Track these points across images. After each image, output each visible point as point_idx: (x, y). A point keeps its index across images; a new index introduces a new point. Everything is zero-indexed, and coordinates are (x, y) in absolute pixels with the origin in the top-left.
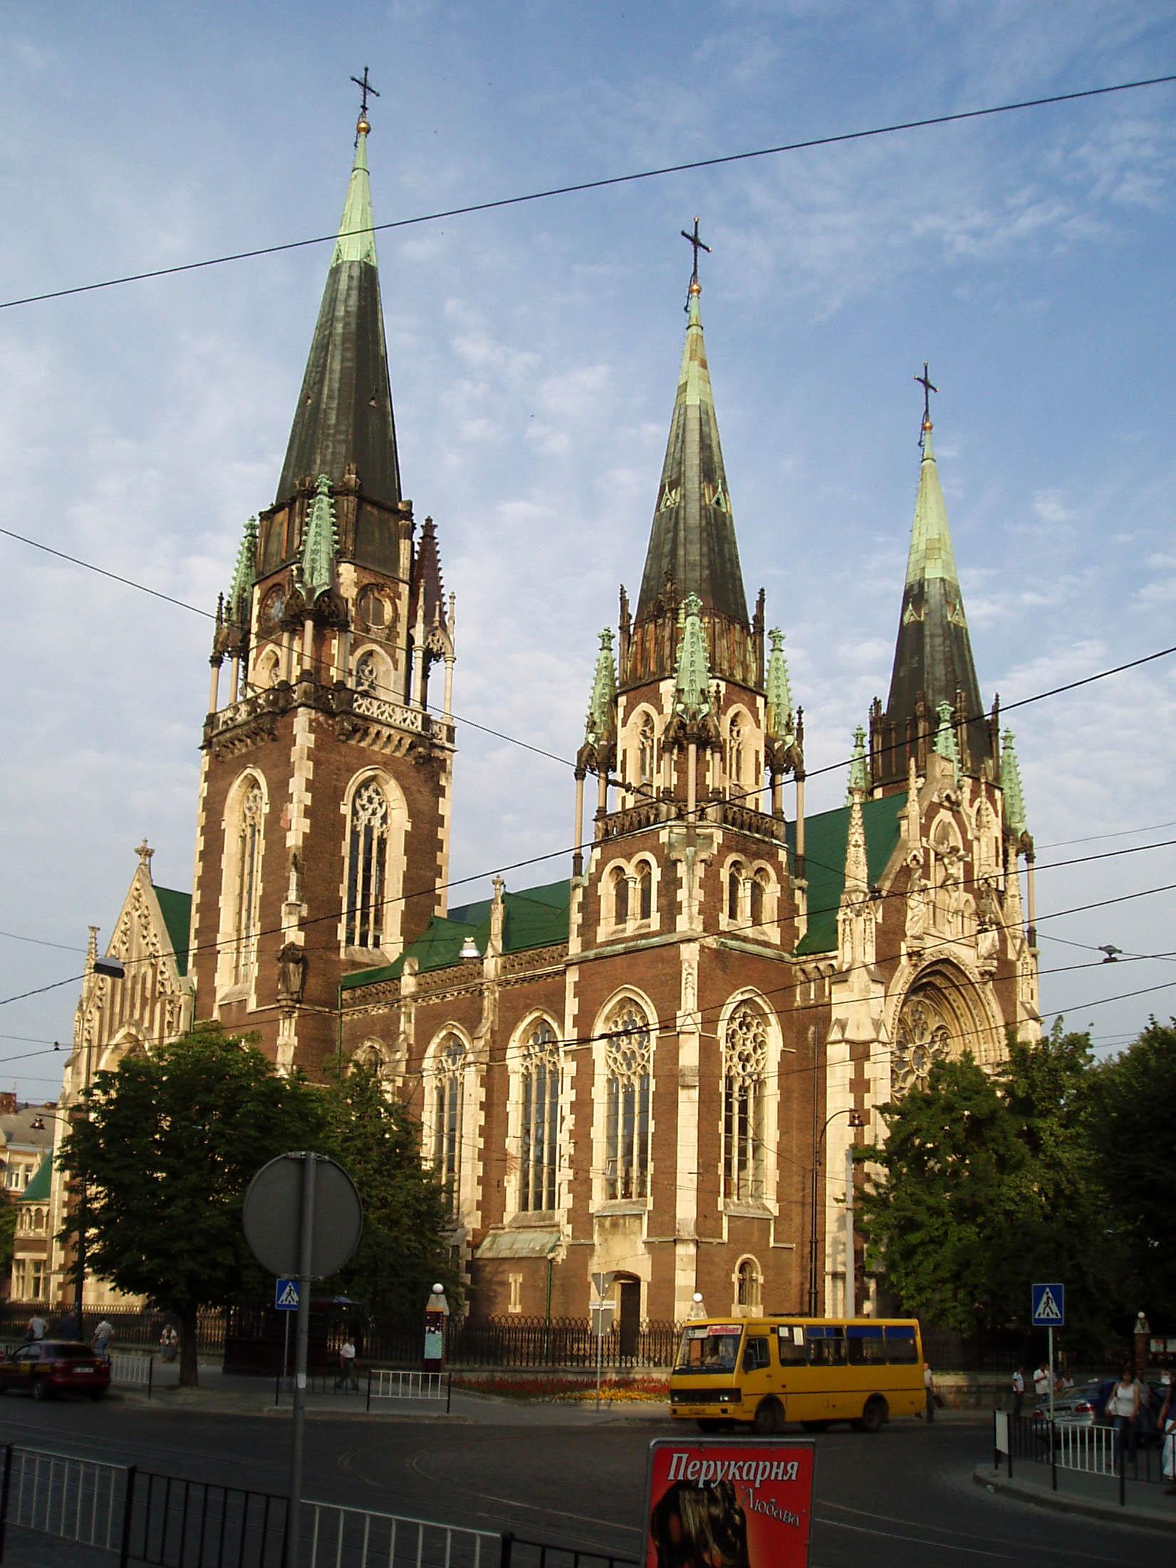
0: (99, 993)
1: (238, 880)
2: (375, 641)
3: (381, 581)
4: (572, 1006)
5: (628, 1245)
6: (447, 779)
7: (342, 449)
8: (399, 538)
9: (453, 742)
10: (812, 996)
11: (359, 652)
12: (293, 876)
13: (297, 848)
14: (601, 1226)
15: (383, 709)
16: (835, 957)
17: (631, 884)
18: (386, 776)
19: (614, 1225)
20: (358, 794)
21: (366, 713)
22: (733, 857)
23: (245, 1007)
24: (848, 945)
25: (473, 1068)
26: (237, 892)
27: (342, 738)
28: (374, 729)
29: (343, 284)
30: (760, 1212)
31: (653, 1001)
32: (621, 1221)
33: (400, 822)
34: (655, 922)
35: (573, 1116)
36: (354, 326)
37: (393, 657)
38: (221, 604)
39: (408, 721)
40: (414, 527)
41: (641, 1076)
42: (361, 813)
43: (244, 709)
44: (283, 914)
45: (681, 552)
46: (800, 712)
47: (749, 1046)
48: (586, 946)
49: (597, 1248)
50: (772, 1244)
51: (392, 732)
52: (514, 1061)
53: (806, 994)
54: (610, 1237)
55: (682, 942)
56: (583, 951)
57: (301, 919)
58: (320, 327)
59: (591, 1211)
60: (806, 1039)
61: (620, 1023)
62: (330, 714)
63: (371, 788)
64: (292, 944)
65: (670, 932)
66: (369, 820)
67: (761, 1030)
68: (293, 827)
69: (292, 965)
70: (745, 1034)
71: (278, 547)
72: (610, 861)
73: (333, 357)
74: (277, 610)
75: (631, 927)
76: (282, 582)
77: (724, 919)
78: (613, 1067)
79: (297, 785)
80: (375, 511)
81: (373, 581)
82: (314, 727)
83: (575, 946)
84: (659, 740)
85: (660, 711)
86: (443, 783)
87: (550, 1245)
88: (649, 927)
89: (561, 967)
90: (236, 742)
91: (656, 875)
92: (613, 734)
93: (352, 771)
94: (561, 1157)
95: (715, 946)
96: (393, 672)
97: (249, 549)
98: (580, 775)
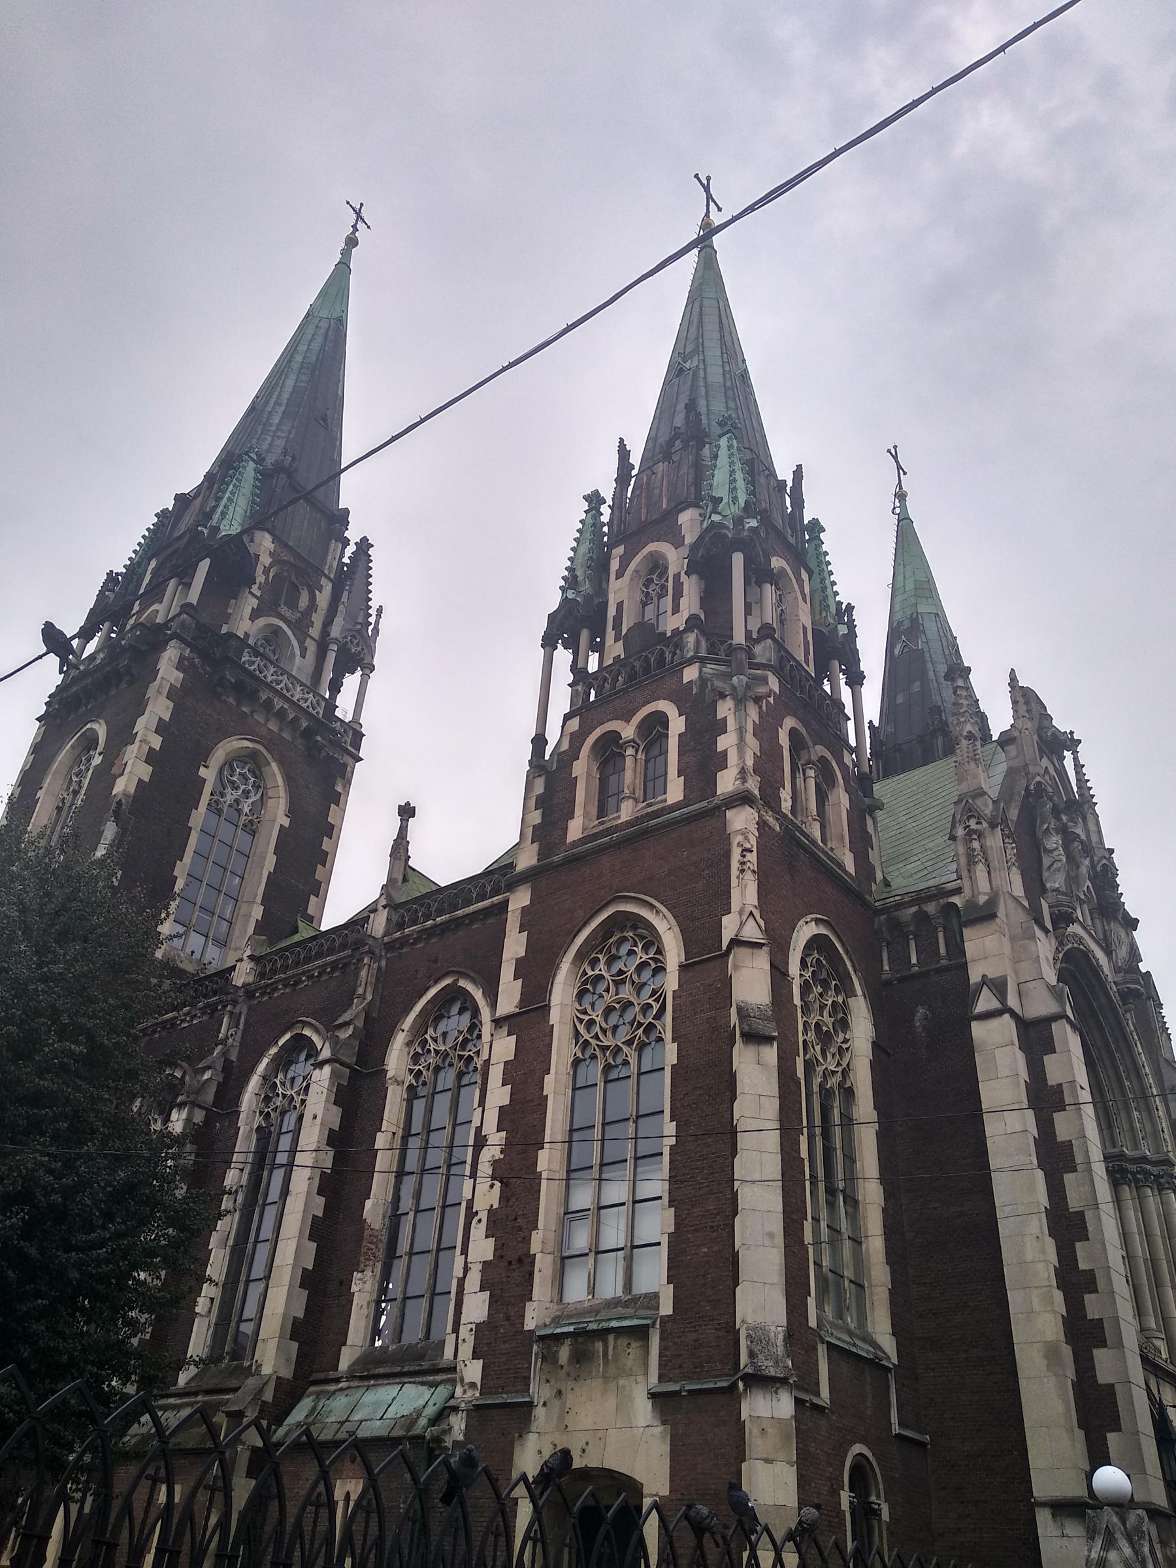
4: (515, 945)
5: (611, 1402)
10: (914, 960)
11: (262, 622)
12: (110, 830)
13: (125, 794)
14: (549, 1358)
15: (280, 678)
17: (630, 751)
18: (268, 756)
19: (581, 1357)
20: (229, 764)
24: (980, 870)
25: (327, 1069)
27: (219, 689)
32: (599, 1345)
33: (278, 814)
34: (675, 791)
37: (301, 644)
39: (309, 703)
40: (346, 542)
42: (229, 790)
45: (702, 403)
49: (539, 1412)
52: (396, 1060)
54: (570, 1384)
56: (539, 860)
59: (530, 1324)
66: (237, 801)
68: (128, 770)
70: (821, 995)
79: (144, 725)
81: (292, 560)
85: (678, 543)
86: (339, 788)
87: (430, 1411)
88: (665, 801)
91: (677, 725)
92: (601, 590)
96: (298, 659)
98: (549, 642)
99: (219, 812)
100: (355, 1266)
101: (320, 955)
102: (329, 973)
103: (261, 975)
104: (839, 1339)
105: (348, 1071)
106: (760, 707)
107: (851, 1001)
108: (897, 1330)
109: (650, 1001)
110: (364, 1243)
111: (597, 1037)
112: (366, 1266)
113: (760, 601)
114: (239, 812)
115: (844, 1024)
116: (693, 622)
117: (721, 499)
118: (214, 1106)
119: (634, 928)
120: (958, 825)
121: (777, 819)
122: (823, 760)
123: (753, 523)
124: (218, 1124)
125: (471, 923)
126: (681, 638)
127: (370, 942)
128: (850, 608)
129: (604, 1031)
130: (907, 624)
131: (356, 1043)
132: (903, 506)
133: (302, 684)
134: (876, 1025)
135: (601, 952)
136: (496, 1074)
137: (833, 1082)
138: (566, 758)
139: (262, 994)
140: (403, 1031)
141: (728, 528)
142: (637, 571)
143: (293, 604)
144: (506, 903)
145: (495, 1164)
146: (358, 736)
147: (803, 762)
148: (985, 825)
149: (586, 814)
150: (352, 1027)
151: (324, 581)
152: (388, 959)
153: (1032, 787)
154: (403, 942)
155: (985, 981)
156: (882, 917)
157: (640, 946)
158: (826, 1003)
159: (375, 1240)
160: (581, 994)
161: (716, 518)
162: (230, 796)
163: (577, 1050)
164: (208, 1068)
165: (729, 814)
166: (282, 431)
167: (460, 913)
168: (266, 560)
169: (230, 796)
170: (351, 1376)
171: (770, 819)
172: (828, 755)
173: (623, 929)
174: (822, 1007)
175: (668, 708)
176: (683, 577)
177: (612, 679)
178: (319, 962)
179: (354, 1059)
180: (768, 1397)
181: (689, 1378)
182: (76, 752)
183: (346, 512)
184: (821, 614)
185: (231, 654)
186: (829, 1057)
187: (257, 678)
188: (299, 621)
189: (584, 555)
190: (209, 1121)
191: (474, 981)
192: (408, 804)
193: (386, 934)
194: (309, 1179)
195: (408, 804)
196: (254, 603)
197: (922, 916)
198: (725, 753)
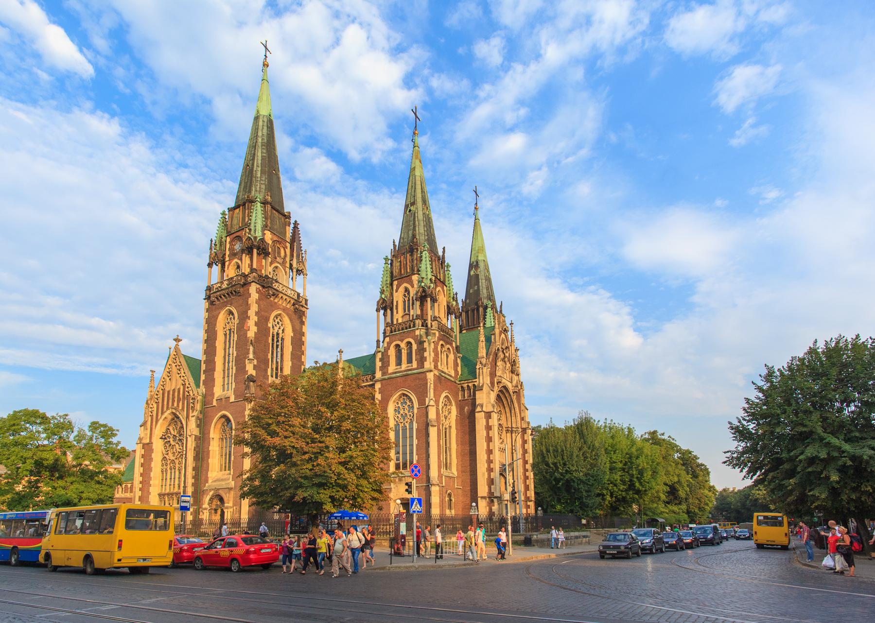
0: (156, 397)
1: (223, 351)
2: (278, 263)
3: (280, 240)
7: (263, 187)
8: (286, 225)
11: (273, 266)
12: (251, 348)
17: (403, 351)
23: (229, 400)
24: (481, 377)
26: (223, 355)
28: (281, 295)
29: (261, 123)
32: (404, 479)
34: (415, 364)
36: (266, 140)
38: (211, 243)
43: (226, 283)
44: (246, 363)
46: (456, 294)
47: (447, 413)
48: (384, 374)
49: (393, 489)
55: (427, 372)
57: (254, 366)
58: (251, 139)
60: (464, 411)
61: (400, 403)
62: (263, 287)
63: (278, 319)
64: (251, 375)
65: (421, 368)
69: (251, 383)
71: (237, 224)
73: (258, 151)
74: (238, 247)
75: (404, 366)
76: (241, 235)
77: (439, 364)
78: (397, 420)
79: (252, 312)
80: (277, 213)
82: (258, 291)
83: (378, 375)
84: (413, 297)
89: (371, 383)
90: (222, 296)
91: (415, 347)
95: (438, 374)
97: (223, 223)
98: (378, 310)
113: (434, 306)
138: (387, 349)
143: (279, 253)
155: (478, 405)
165: (427, 374)
168: (270, 242)
182: (225, 315)
183: (289, 213)
187: (277, 291)
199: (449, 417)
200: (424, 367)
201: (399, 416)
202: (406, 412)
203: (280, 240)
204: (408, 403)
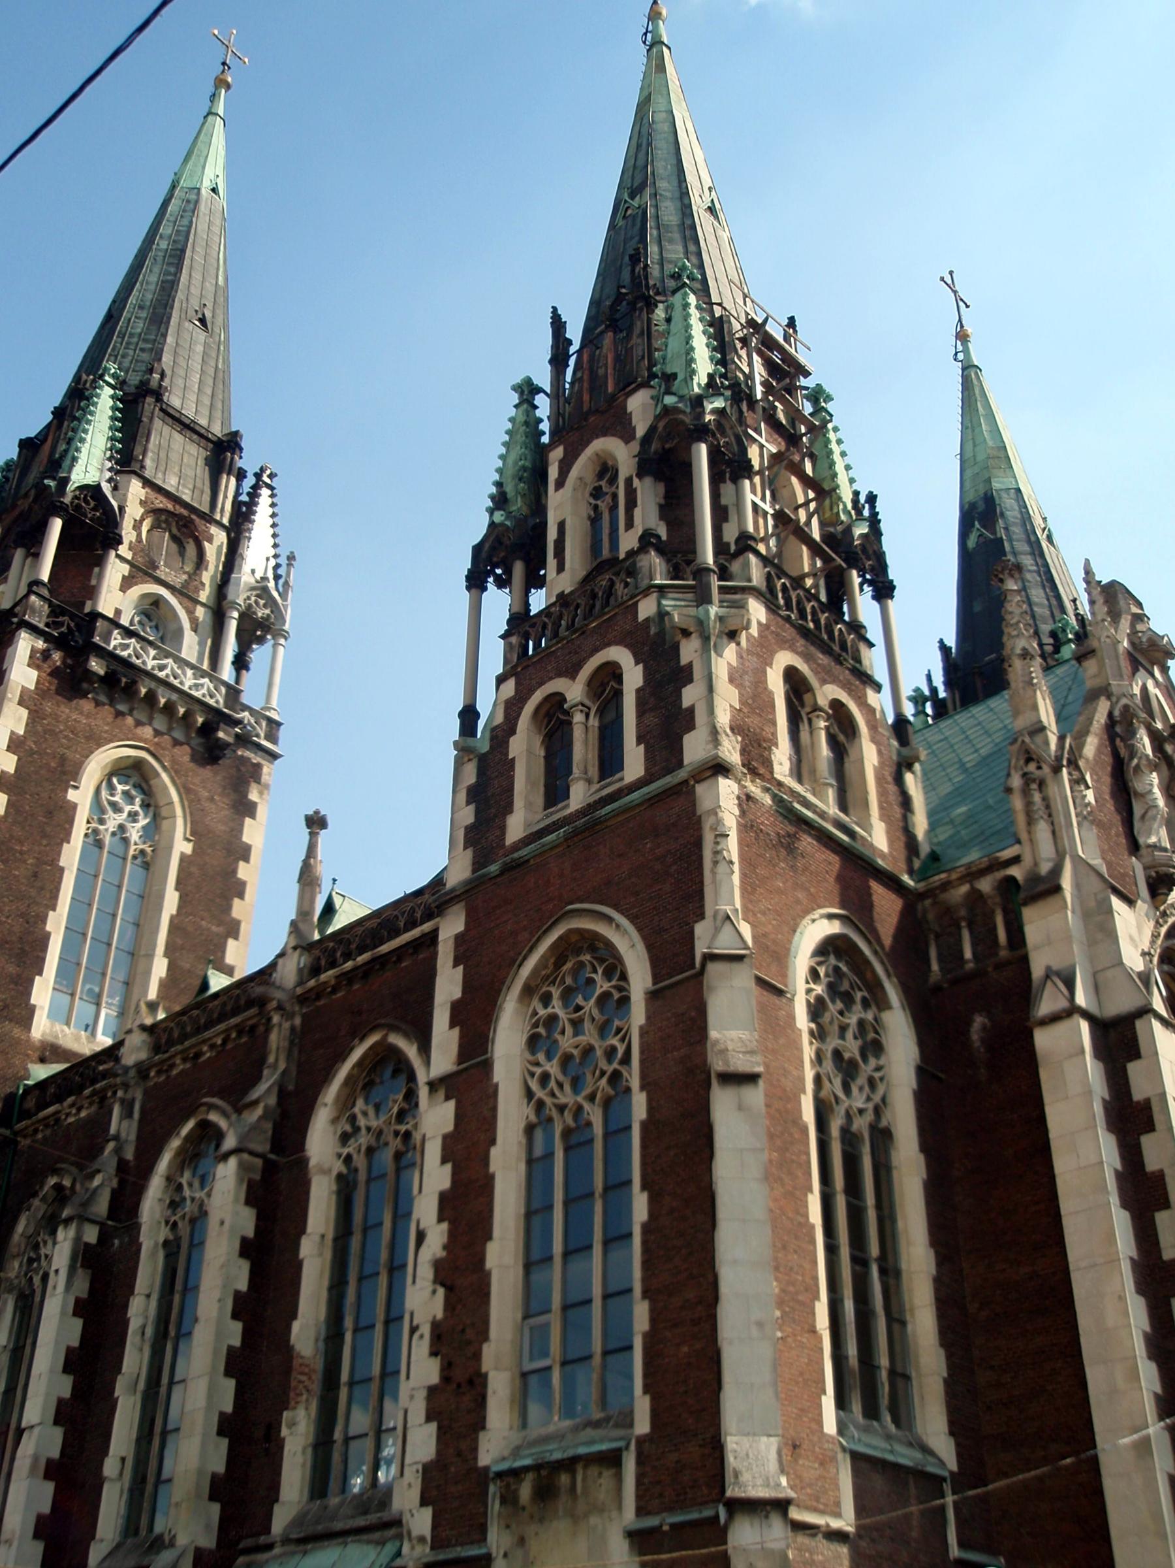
6: (261, 793)
9: (274, 741)
10: (968, 954)
14: (509, 1499)
16: (1016, 860)
17: (578, 718)
19: (545, 1493)
21: (134, 660)
22: (784, 659)
24: (1042, 830)
25: (233, 1162)
30: (918, 1455)
31: (633, 919)
32: (564, 1479)
34: (634, 763)
35: (445, 1226)
37: (190, 612)
41: (607, 1103)
47: (852, 1047)
50: (955, 1551)
51: (174, 697)
53: (952, 956)
56: (474, 871)
65: (669, 771)
66: (122, 828)
67: (869, 1016)
70: (841, 1013)
72: (531, 691)
75: (579, 795)
78: (540, 1093)
82: (37, 660)
86: (253, 796)
88: (622, 779)
89: (427, 927)
91: (633, 677)
92: (538, 508)
93: (96, 741)
94: (413, 1330)
98: (476, 581)
99: (99, 844)
100: (284, 1404)
101: (222, 1018)
102: (235, 1039)
103: (156, 1048)
104: (868, 1445)
105: (259, 1162)
106: (738, 644)
107: (886, 1016)
108: (956, 1428)
109: (615, 1041)
110: (294, 1374)
111: (553, 1095)
112: (297, 1403)
114: (126, 841)
115: (874, 1047)
116: (648, 540)
117: (674, 376)
118: (110, 1217)
119: (593, 949)
120: (1013, 772)
121: (767, 790)
122: (837, 705)
123: (719, 403)
124: (116, 1242)
125: (399, 960)
126: (634, 563)
127: (278, 995)
128: (872, 499)
129: (560, 1085)
130: (981, 507)
131: (269, 1126)
132: (966, 351)
133: (193, 667)
134: (922, 1043)
135: (553, 982)
136: (433, 1151)
137: (861, 1124)
138: (502, 734)
139: (159, 1073)
140: (326, 1105)
141: (684, 412)
142: (581, 479)
144: (435, 933)
145: (438, 1265)
146: (274, 725)
147: (808, 709)
148: (1046, 769)
149: (529, 805)
150: (262, 1105)
151: (214, 530)
152: (305, 1017)
153: (1117, 713)
154: (318, 993)
155: (1049, 974)
156: (928, 902)
157: (600, 971)
158: (847, 1021)
159: (307, 1370)
160: (533, 1042)
161: (669, 400)
162: (113, 821)
163: (529, 1112)
164: (99, 1171)
165: (700, 789)
166: (145, 341)
167: (385, 948)
169: (113, 821)
170: (286, 1541)
171: (755, 789)
172: (844, 697)
173: (578, 952)
174: (843, 1029)
175: (620, 655)
176: (636, 482)
177: (553, 624)
178: (222, 1027)
179: (268, 1147)
180: (757, 1522)
181: (670, 1509)
184: (831, 509)
185: (97, 639)
186: (855, 1090)
188: (186, 584)
189: (516, 463)
190: (104, 1237)
191: (407, 1035)
192: (317, 812)
193: (301, 983)
194: (219, 1300)
195: (317, 812)
196: (125, 569)
197: (976, 897)
198: (691, 710)
199: (867, 1069)
200: (680, 764)
201: (553, 1068)
202: (589, 1036)
203: (185, 512)
204: (602, 985)
